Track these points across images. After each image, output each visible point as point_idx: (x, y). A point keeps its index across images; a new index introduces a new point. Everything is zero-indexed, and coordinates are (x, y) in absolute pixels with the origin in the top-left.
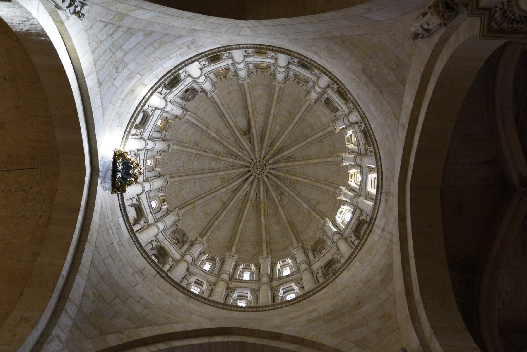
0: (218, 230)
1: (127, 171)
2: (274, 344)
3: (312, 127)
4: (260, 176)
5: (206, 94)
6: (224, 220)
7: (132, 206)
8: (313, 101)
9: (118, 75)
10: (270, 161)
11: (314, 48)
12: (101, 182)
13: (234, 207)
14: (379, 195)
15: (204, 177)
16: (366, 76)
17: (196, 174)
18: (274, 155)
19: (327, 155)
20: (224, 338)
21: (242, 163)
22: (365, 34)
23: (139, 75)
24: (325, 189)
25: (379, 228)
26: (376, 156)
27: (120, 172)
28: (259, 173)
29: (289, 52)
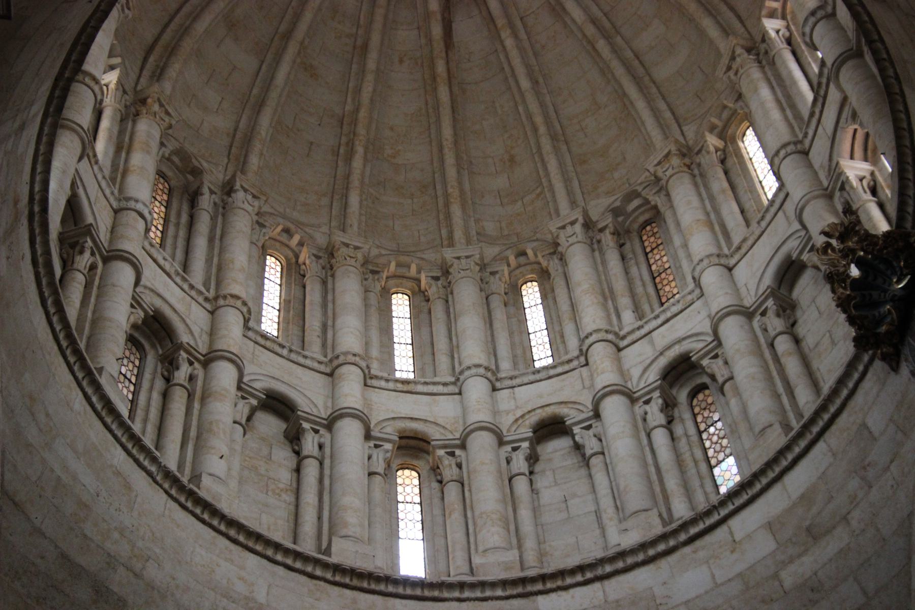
5: (588, 225)
8: (240, 195)
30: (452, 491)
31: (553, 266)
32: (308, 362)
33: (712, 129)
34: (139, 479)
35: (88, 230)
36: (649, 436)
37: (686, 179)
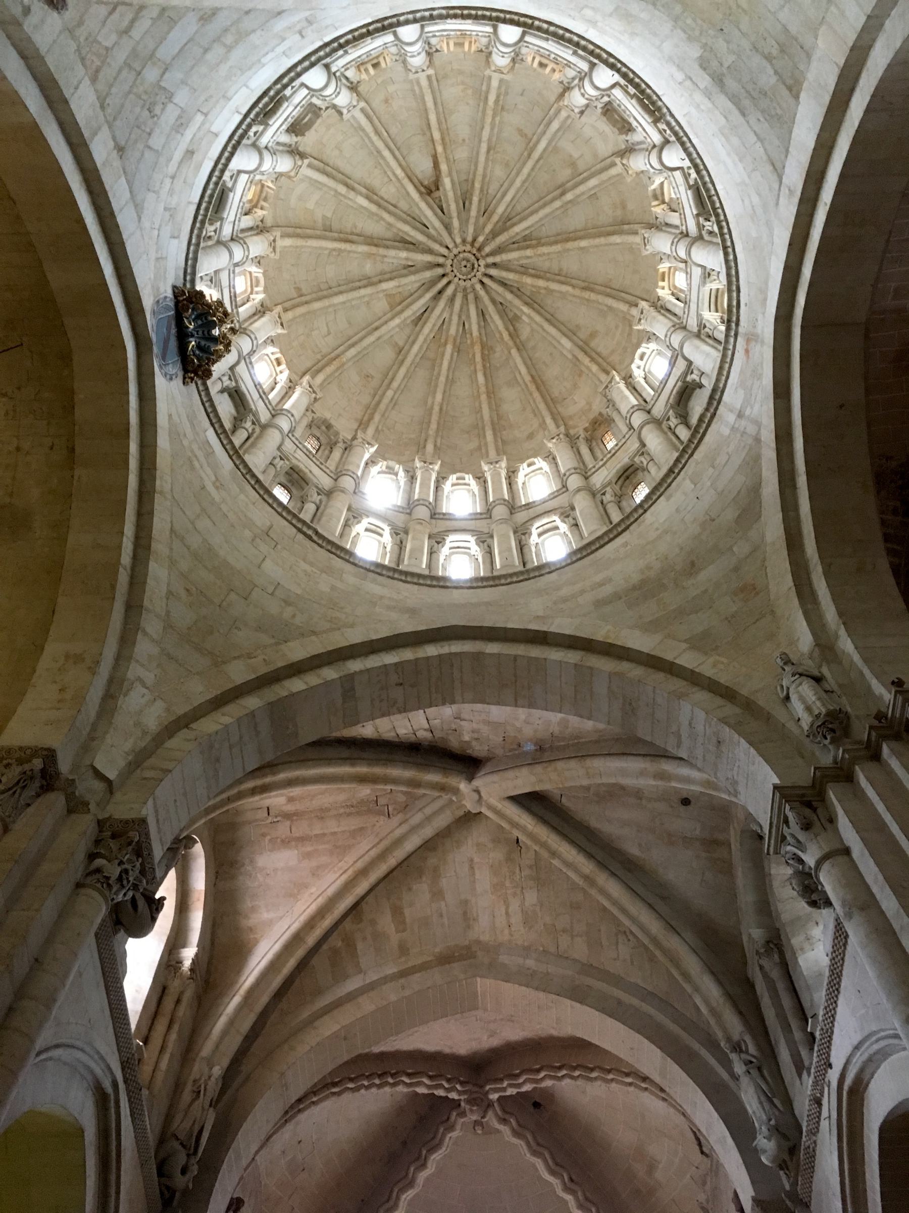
0: (393, 408)
1: (206, 333)
2: (535, 652)
3: (573, 165)
4: (468, 284)
5: (340, 113)
6: (402, 387)
7: (222, 391)
8: (577, 110)
9: (155, 124)
10: (487, 249)
11: (588, 13)
12: (160, 367)
13: (420, 355)
14: (732, 340)
15: (353, 299)
16: (709, 75)
17: (336, 294)
18: (494, 234)
19: (609, 229)
20: (442, 647)
21: (428, 258)
23: (199, 114)
24: (607, 306)
25: (731, 411)
26: (726, 254)
27: (192, 336)
28: (465, 277)
29: (530, 21)
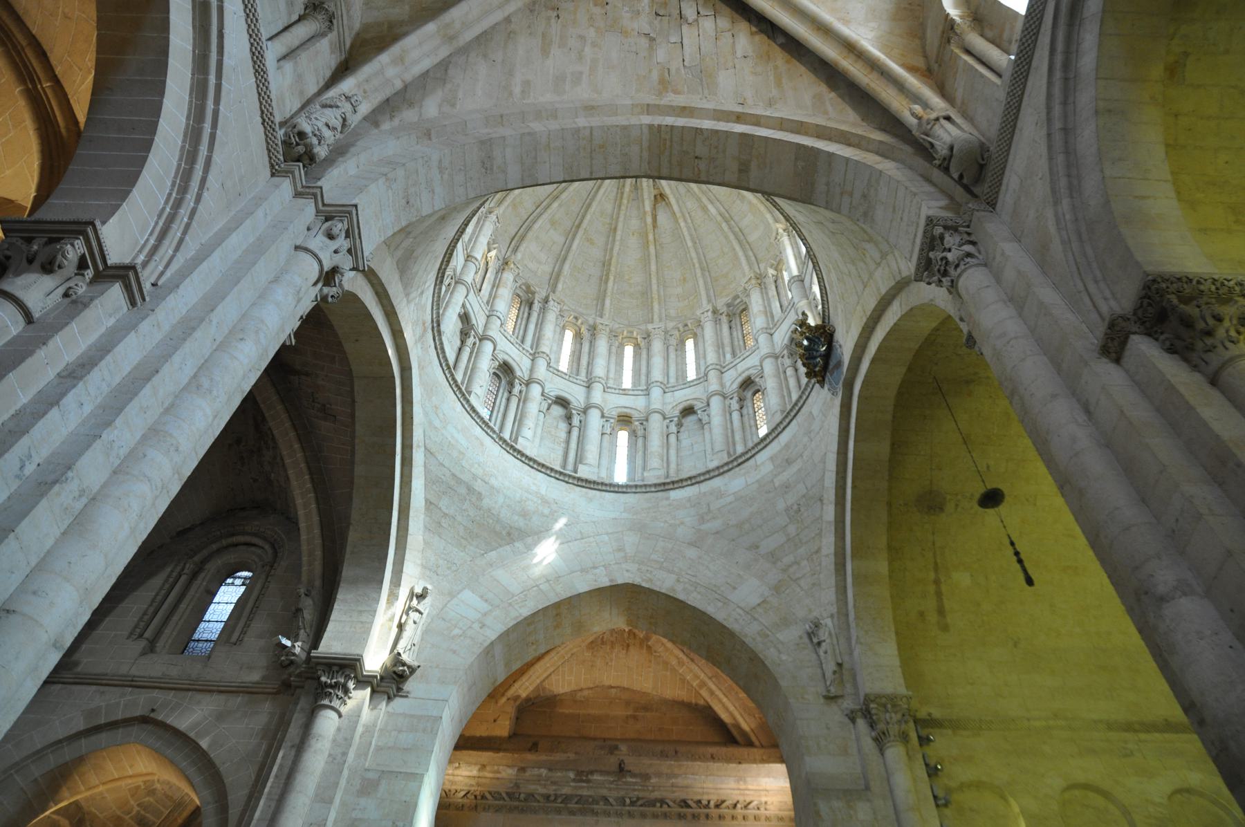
5: (715, 312)
8: (551, 303)
22: (483, 555)
30: (640, 441)
31: (699, 331)
32: (578, 382)
33: (771, 267)
34: (488, 441)
35: (472, 327)
36: (731, 415)
37: (758, 290)
